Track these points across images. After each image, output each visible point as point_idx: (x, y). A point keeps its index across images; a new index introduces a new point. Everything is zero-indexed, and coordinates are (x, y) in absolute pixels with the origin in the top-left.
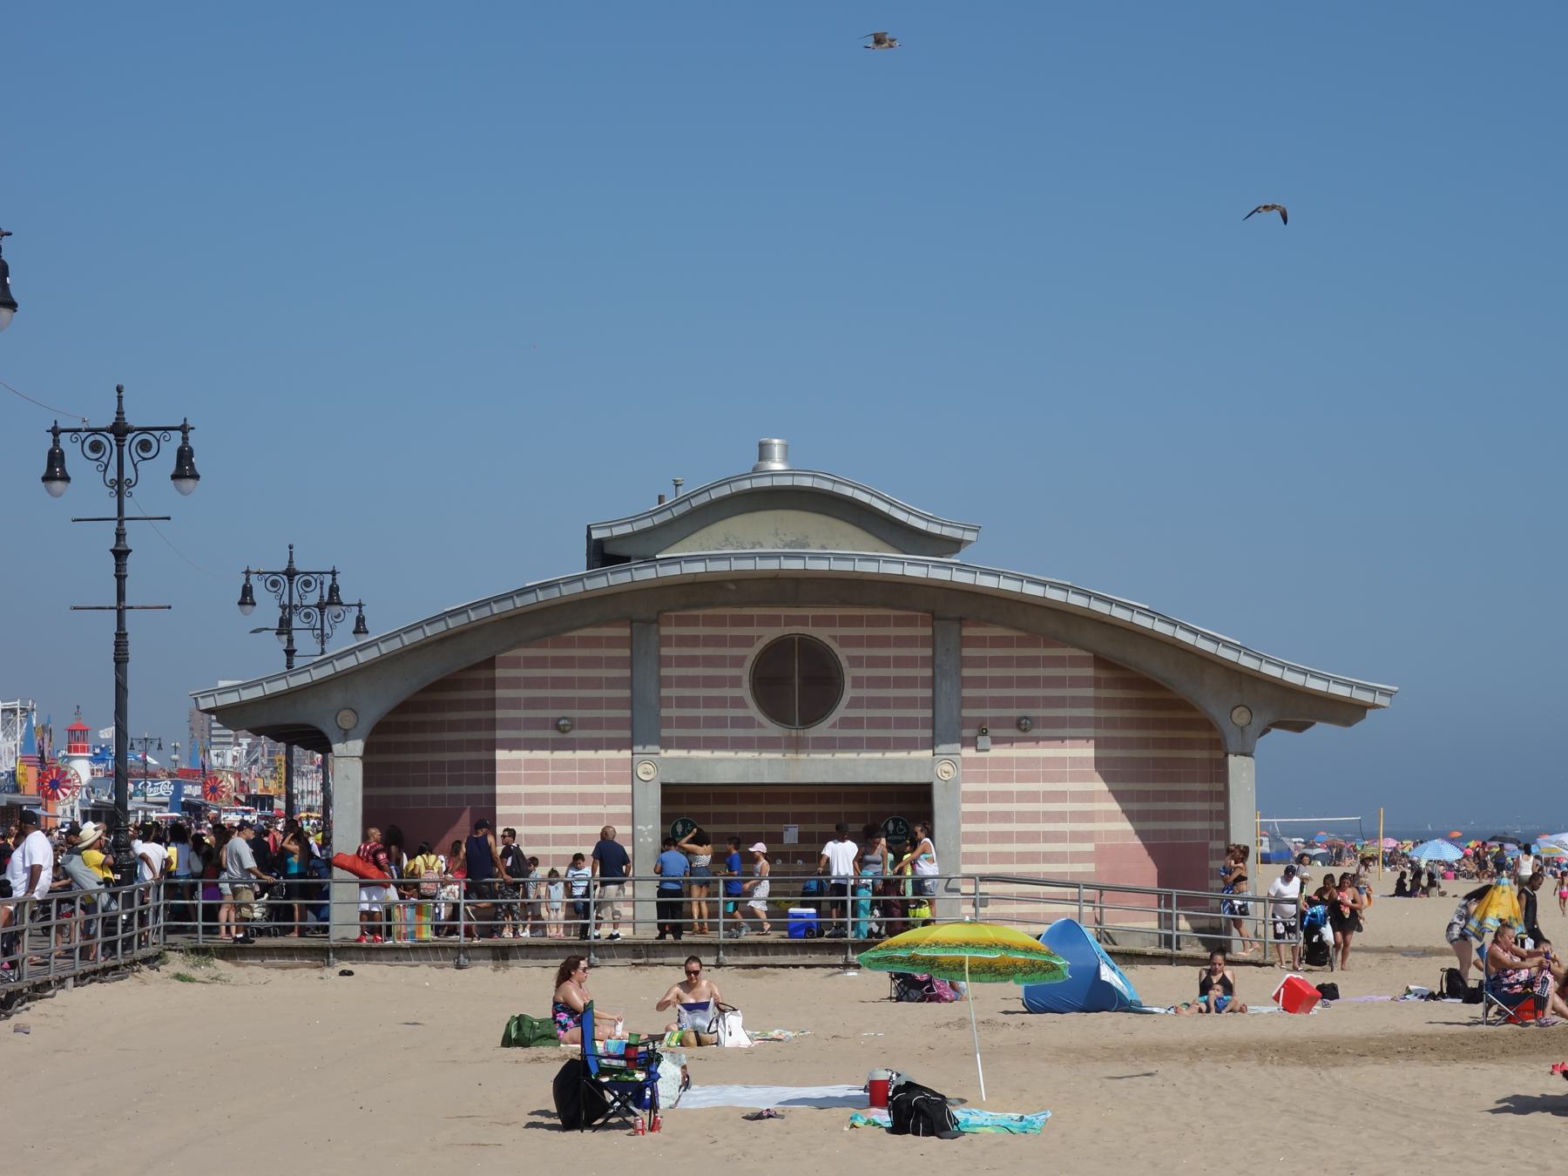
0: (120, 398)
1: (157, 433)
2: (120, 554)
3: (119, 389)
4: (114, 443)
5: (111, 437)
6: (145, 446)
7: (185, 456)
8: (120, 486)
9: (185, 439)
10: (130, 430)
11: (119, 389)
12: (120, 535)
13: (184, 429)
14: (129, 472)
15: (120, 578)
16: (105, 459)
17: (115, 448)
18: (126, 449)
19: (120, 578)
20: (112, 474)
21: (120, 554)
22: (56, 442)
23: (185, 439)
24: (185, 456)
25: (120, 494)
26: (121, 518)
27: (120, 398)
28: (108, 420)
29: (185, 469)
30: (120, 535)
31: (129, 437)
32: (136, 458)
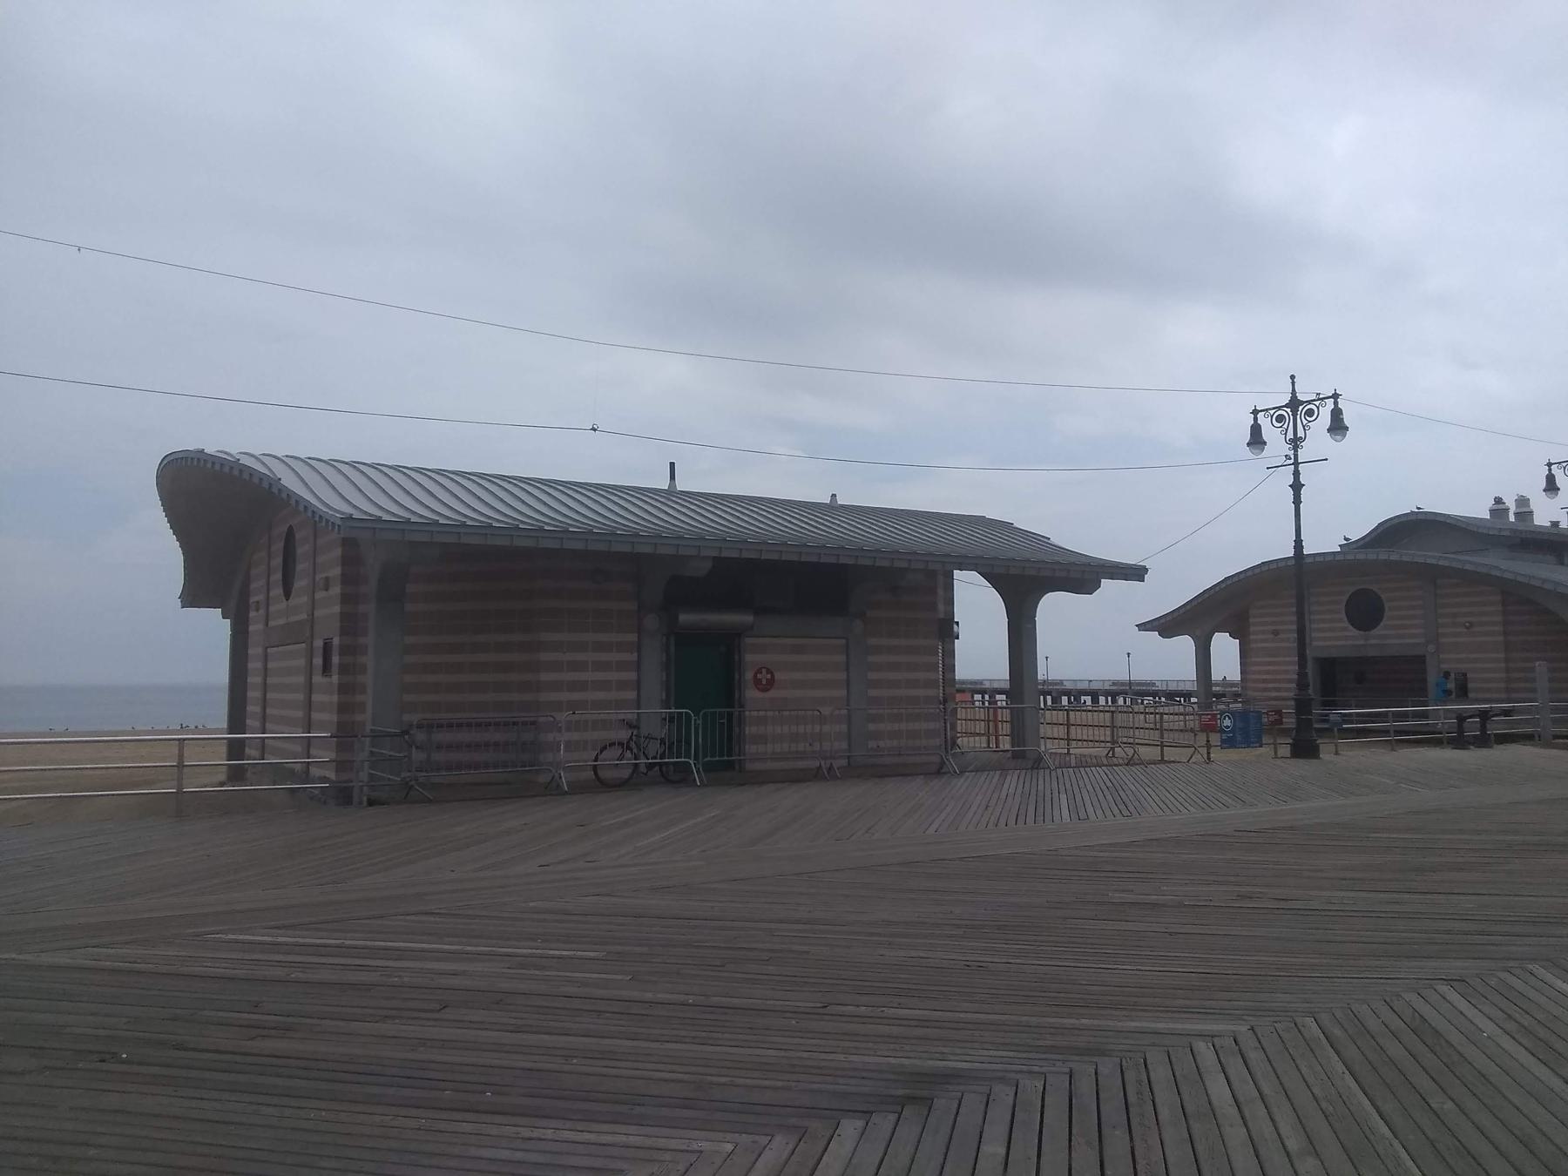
0: (1293, 383)
1: (1317, 403)
2: (1297, 487)
3: (1293, 377)
4: (1290, 413)
5: (1289, 410)
6: (1310, 413)
7: (1337, 414)
8: (1296, 443)
9: (1336, 403)
10: (1302, 403)
11: (1293, 377)
12: (1296, 474)
13: (1335, 396)
14: (1300, 433)
15: (1297, 501)
16: (1285, 426)
17: (1291, 417)
18: (1298, 416)
19: (1297, 501)
20: (1290, 435)
21: (1297, 487)
22: (1256, 419)
23: (1336, 403)
24: (1337, 414)
25: (1296, 448)
26: (1296, 464)
27: (1293, 383)
28: (1286, 399)
29: (1338, 426)
30: (1296, 474)
31: (1301, 408)
32: (1305, 422)
